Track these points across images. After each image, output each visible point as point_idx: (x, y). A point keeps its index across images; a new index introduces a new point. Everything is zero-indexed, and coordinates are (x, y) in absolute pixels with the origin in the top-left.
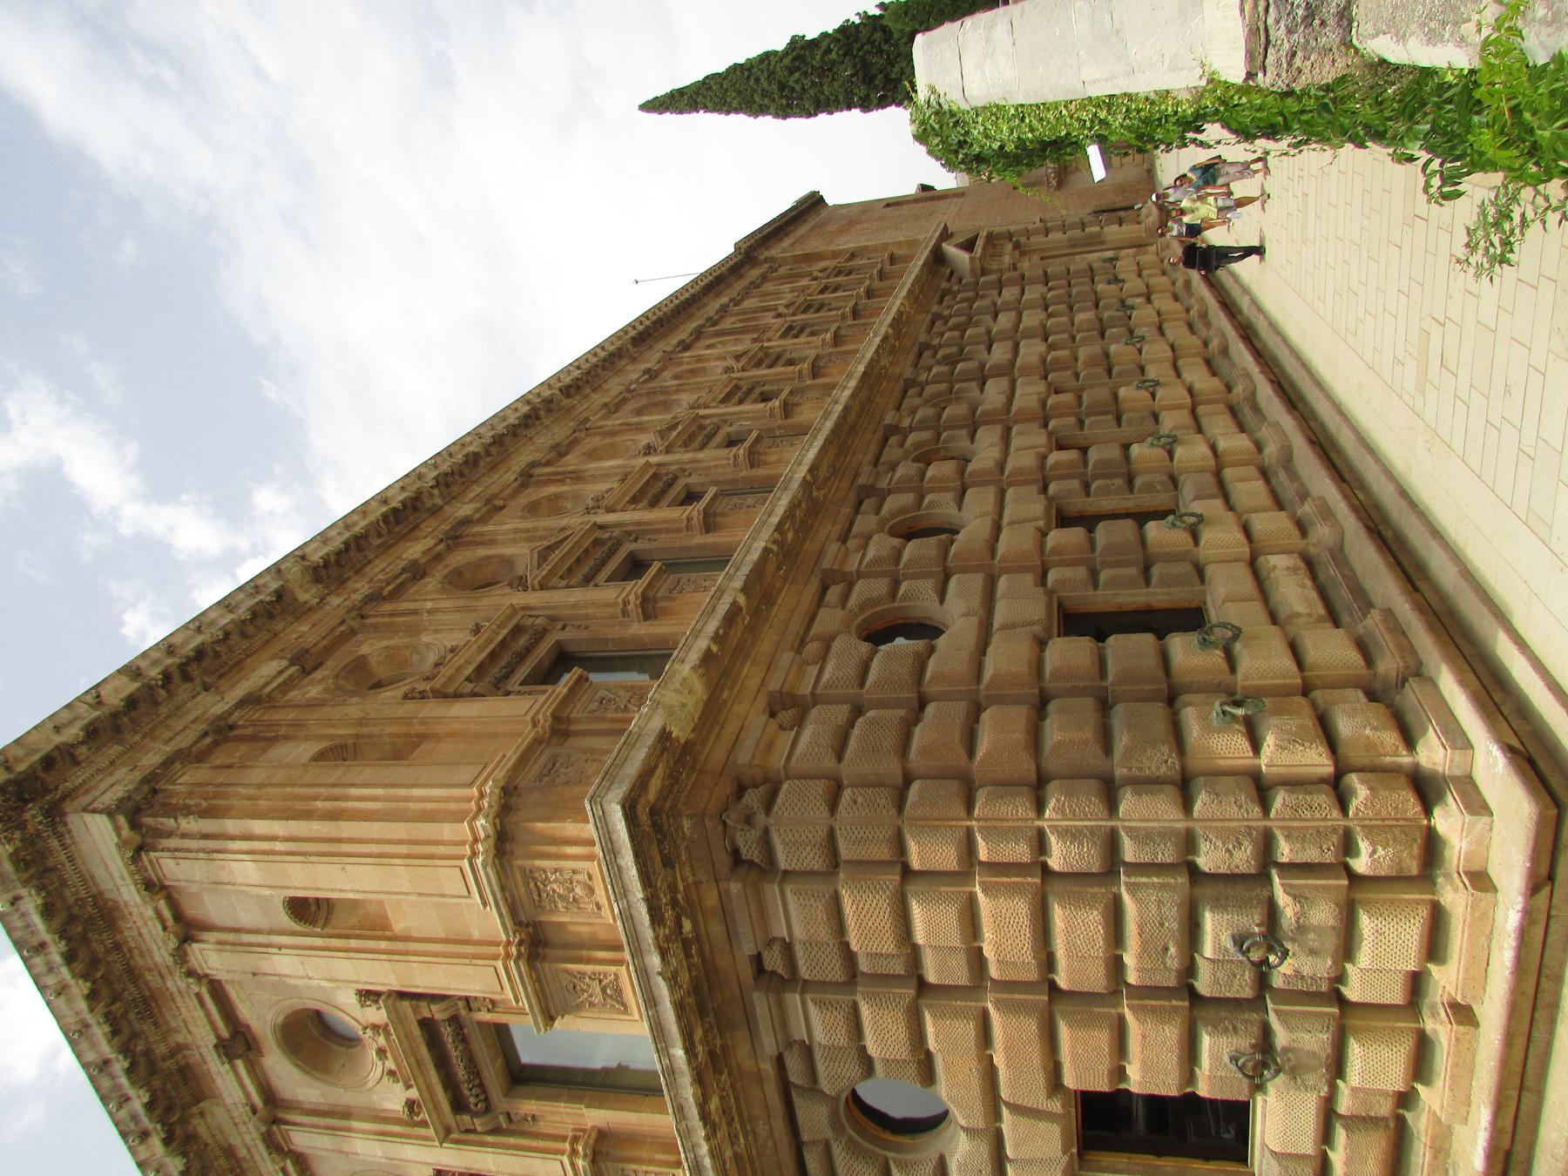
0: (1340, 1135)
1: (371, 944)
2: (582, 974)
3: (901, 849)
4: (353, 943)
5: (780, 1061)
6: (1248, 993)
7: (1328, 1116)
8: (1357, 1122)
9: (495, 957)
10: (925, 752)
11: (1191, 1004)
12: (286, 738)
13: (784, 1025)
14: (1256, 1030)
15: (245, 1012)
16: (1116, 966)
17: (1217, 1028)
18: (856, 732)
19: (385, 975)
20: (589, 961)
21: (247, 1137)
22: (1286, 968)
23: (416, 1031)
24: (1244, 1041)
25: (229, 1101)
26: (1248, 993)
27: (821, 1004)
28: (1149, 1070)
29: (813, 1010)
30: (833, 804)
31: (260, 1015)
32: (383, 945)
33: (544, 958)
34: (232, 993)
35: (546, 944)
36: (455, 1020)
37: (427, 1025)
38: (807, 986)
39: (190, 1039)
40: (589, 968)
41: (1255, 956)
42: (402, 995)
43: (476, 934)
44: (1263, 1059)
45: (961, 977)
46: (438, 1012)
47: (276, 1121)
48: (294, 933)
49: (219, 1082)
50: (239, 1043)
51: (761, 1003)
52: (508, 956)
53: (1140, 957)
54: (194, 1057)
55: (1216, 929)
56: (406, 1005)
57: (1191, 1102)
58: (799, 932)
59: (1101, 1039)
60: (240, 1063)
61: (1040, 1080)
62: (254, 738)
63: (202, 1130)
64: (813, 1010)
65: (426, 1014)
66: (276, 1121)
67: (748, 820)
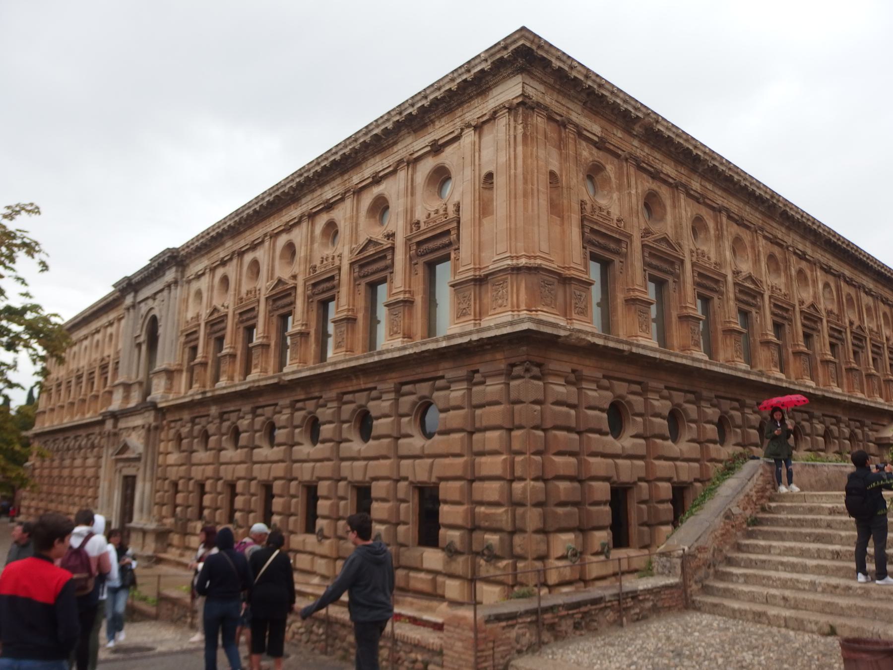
0: (430, 577)
1: (477, 210)
2: (470, 300)
3: (520, 427)
4: (477, 202)
5: (442, 377)
6: (474, 549)
7: (436, 573)
8: (434, 581)
9: (475, 264)
10: (555, 436)
11: (473, 528)
12: (561, 154)
13: (455, 381)
14: (462, 550)
15: (449, 150)
16: (481, 503)
17: (462, 537)
18: (564, 409)
19: (466, 216)
20: (475, 303)
21: (401, 151)
22: (482, 562)
23: (446, 228)
24: (458, 545)
25: (414, 144)
26: (474, 549)
27: (464, 395)
28: (448, 513)
29: (461, 392)
30: (536, 402)
31: (449, 157)
32: (477, 215)
33: (475, 285)
34: (456, 145)
35: (480, 285)
36: (450, 244)
37: (448, 232)
38: (469, 390)
39: (437, 127)
40: (472, 303)
41: (486, 552)
42: (459, 222)
43: (483, 255)
44: (452, 552)
45: (476, 448)
46: (453, 237)
47: (408, 165)
48: (480, 175)
49: (422, 140)
50: (437, 148)
51: (462, 372)
52: (475, 269)
53: (484, 512)
54: (430, 129)
55: (493, 539)
56: (455, 224)
57: (438, 527)
58: (489, 388)
59: (456, 497)
60: (428, 149)
61: (441, 475)
62: (561, 139)
63: (402, 133)
64: (461, 392)
65: (452, 232)
66: (408, 165)
67: (527, 370)
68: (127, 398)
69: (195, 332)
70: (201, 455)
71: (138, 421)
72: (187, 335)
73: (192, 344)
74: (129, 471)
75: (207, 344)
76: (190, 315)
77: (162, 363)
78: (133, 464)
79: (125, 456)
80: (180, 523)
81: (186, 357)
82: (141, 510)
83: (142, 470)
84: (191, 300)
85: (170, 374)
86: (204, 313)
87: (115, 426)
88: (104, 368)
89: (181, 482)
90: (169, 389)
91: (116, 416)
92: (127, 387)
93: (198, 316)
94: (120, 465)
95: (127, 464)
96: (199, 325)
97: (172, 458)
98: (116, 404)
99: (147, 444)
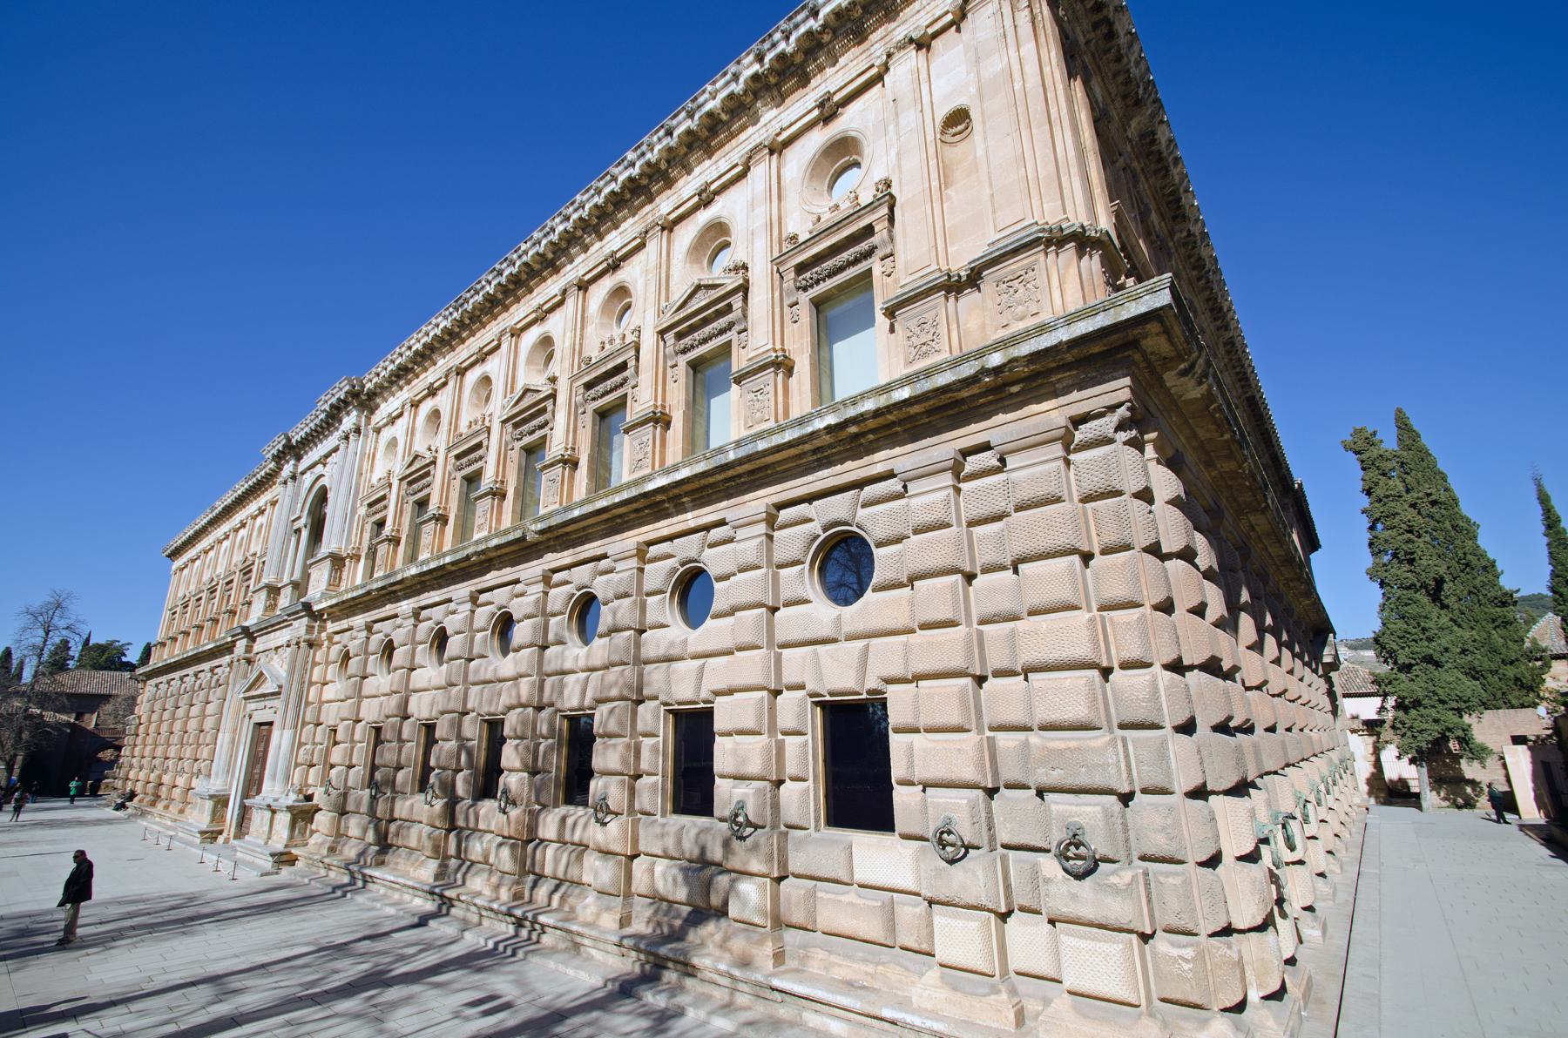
68: (271, 607)
69: (383, 498)
70: (381, 681)
71: (282, 637)
72: (370, 505)
73: (378, 516)
74: (261, 717)
75: (399, 512)
76: (379, 472)
77: (325, 549)
78: (269, 703)
79: (258, 692)
80: (334, 793)
81: (367, 536)
82: (274, 778)
83: (281, 712)
84: (379, 455)
85: (337, 561)
86: (399, 469)
87: (249, 649)
88: (247, 572)
89: (340, 730)
90: (334, 581)
91: (249, 634)
92: (274, 591)
93: (389, 473)
94: (252, 706)
95: (261, 705)
96: (390, 485)
97: (330, 692)
98: (255, 616)
99: (292, 671)
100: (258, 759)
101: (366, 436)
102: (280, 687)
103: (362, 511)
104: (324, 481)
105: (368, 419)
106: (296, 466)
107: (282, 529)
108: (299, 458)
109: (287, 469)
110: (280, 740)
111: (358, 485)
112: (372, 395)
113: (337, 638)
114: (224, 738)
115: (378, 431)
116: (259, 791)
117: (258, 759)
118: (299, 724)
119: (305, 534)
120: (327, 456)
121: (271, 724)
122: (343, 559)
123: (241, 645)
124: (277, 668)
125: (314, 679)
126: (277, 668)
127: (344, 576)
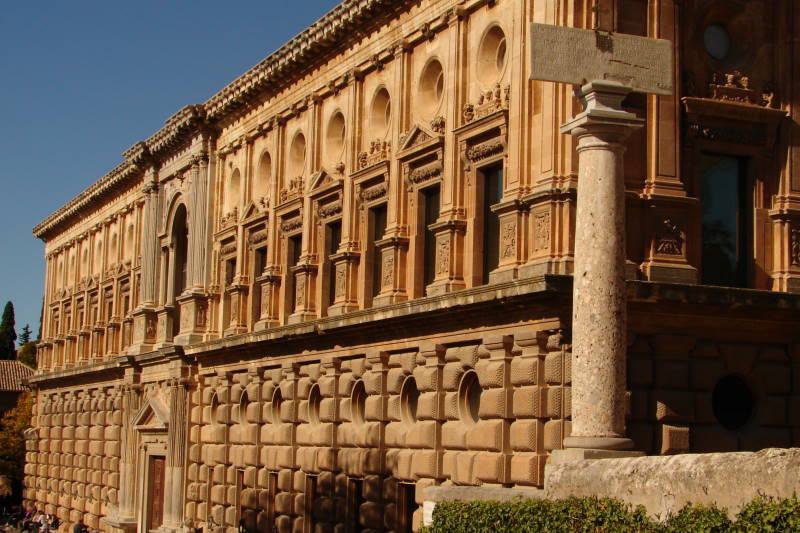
76: (227, 209)
87: (137, 379)
94: (146, 438)
100: (156, 491)
101: (214, 163)
102: (166, 424)
103: (217, 247)
104: (182, 199)
105: (214, 147)
106: (156, 174)
107: (151, 248)
108: (158, 167)
109: (149, 177)
110: (172, 475)
111: (211, 218)
112: (214, 120)
113: (207, 381)
114: (125, 467)
115: (223, 157)
116: (160, 523)
117: (156, 491)
118: (185, 463)
119: (172, 254)
120: (183, 171)
121: (163, 458)
122: (205, 299)
123: (129, 372)
124: (162, 402)
125: (193, 420)
126: (162, 402)
127: (208, 317)
